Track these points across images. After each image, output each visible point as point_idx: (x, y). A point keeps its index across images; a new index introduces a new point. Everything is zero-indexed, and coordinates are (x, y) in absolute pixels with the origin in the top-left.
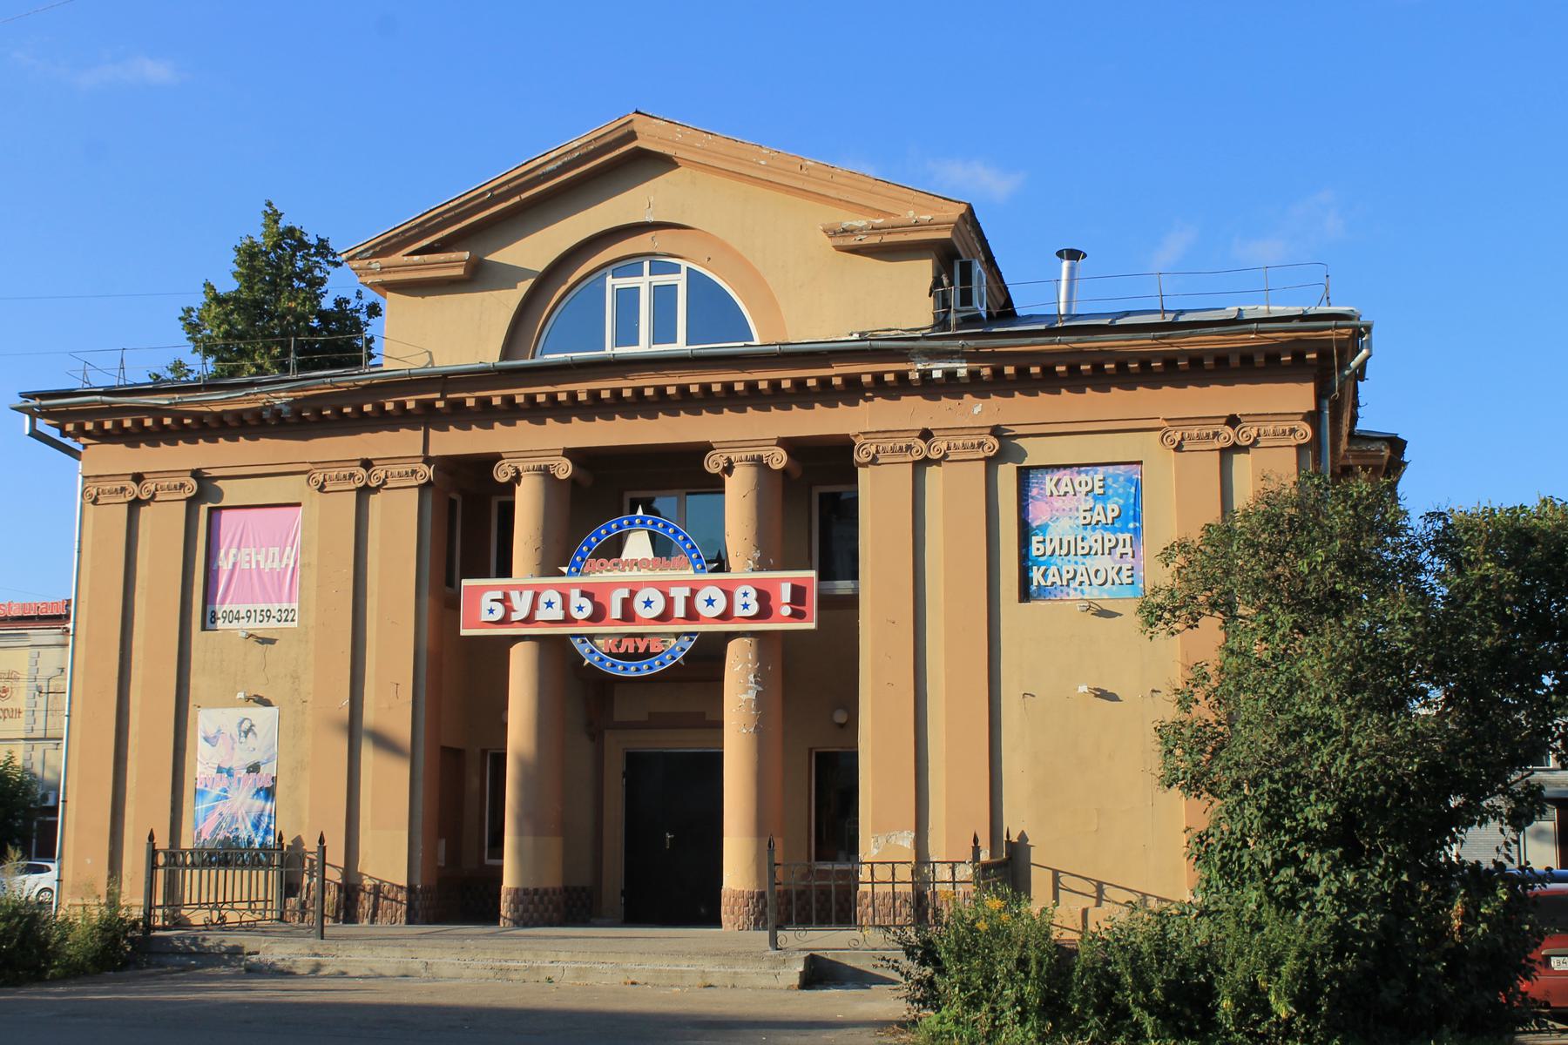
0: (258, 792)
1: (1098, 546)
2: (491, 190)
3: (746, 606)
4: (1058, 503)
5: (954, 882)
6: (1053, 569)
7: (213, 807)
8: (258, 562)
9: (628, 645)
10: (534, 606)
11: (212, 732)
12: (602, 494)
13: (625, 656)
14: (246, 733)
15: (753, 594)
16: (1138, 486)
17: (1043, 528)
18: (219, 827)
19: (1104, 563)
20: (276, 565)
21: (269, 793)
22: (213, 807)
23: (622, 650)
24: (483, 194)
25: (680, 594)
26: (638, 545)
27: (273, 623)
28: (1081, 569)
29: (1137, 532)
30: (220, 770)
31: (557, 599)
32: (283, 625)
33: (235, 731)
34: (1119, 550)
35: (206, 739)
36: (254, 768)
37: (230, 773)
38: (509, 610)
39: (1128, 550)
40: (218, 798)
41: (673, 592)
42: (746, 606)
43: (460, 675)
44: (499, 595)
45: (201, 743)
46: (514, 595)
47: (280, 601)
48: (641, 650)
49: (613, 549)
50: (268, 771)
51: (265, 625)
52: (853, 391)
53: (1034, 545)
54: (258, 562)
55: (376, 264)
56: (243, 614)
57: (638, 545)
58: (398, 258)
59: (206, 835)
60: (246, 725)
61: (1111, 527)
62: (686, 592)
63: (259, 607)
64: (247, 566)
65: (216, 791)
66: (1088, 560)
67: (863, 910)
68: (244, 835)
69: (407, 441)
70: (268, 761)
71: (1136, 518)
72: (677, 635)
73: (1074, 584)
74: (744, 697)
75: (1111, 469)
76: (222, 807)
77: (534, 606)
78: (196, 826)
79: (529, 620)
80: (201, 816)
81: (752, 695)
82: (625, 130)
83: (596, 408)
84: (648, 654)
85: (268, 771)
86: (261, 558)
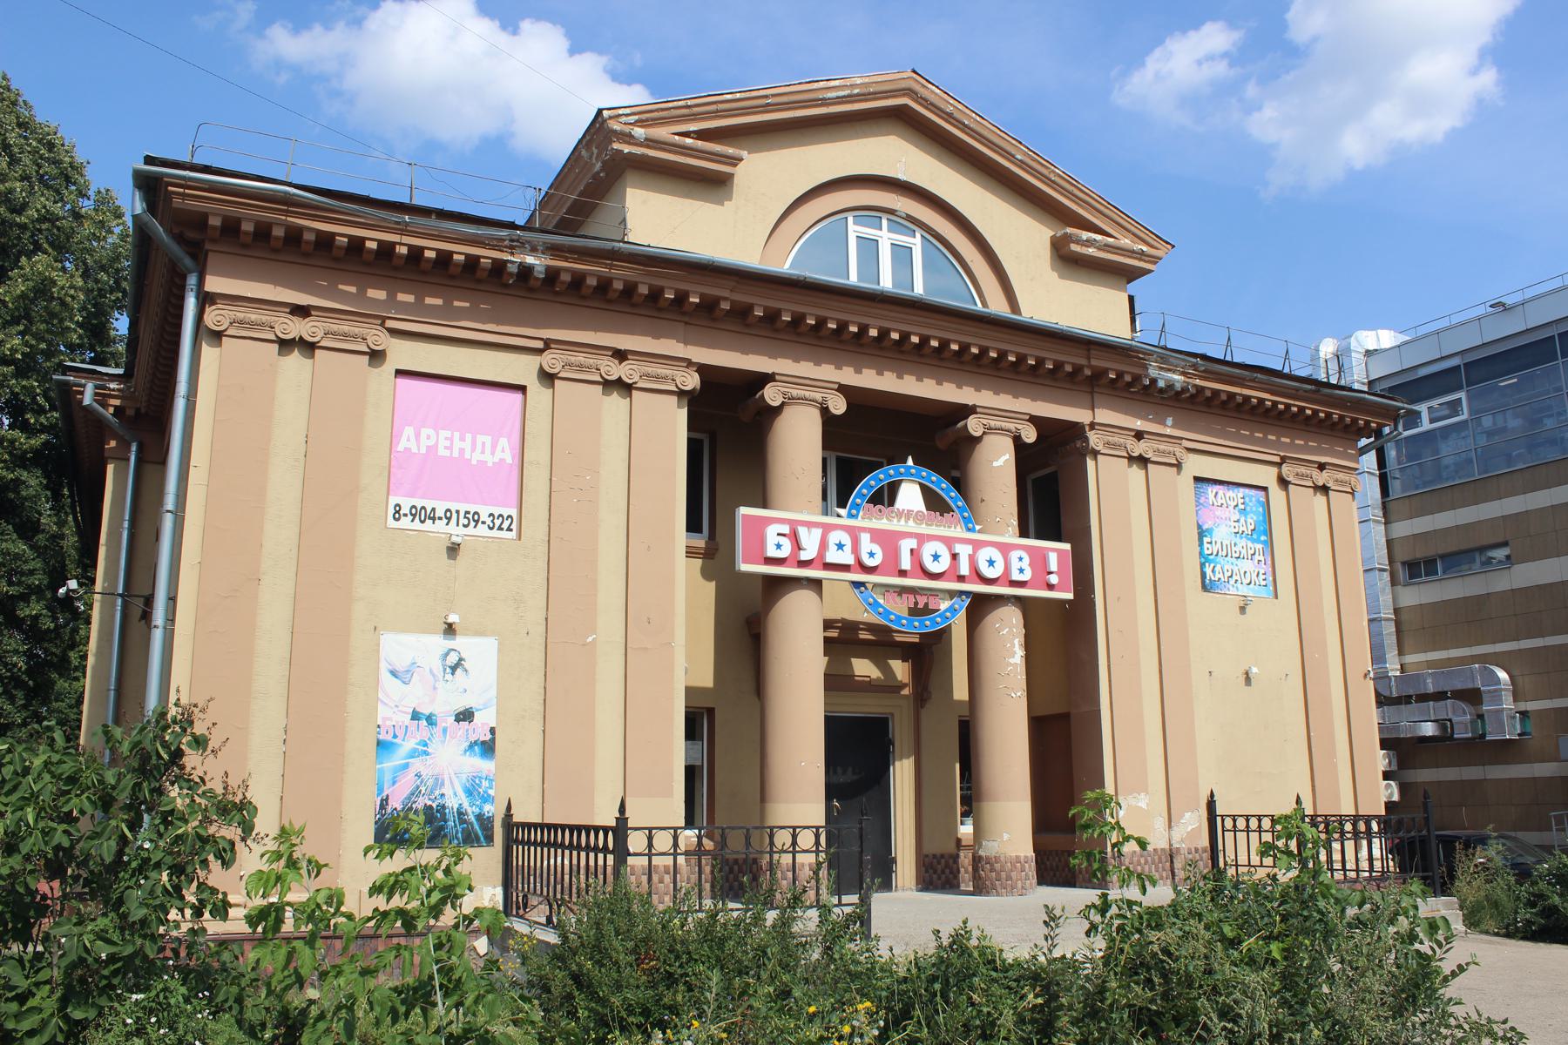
0: (471, 746)
3: (1021, 571)
4: (1219, 512)
5: (650, 855)
6: (1218, 568)
7: (406, 766)
8: (462, 451)
10: (823, 546)
14: (454, 669)
15: (1026, 559)
17: (1210, 531)
18: (416, 792)
19: (1247, 565)
21: (488, 748)
22: (406, 766)
24: (766, 97)
26: (910, 497)
27: (482, 530)
30: (416, 716)
31: (846, 539)
32: (495, 533)
33: (437, 666)
35: (394, 673)
36: (465, 716)
37: (430, 720)
38: (798, 546)
40: (413, 754)
41: (958, 548)
44: (786, 529)
45: (385, 676)
46: (802, 531)
48: (921, 606)
49: (885, 497)
50: (485, 719)
51: (471, 530)
57: (910, 497)
58: (663, 133)
59: (396, 803)
60: (453, 659)
61: (1250, 537)
62: (969, 549)
63: (463, 508)
65: (409, 744)
68: (452, 803)
72: (952, 594)
73: (1232, 581)
75: (1247, 491)
76: (417, 765)
77: (823, 546)
78: (381, 790)
80: (388, 777)
85: (485, 719)
86: (467, 445)
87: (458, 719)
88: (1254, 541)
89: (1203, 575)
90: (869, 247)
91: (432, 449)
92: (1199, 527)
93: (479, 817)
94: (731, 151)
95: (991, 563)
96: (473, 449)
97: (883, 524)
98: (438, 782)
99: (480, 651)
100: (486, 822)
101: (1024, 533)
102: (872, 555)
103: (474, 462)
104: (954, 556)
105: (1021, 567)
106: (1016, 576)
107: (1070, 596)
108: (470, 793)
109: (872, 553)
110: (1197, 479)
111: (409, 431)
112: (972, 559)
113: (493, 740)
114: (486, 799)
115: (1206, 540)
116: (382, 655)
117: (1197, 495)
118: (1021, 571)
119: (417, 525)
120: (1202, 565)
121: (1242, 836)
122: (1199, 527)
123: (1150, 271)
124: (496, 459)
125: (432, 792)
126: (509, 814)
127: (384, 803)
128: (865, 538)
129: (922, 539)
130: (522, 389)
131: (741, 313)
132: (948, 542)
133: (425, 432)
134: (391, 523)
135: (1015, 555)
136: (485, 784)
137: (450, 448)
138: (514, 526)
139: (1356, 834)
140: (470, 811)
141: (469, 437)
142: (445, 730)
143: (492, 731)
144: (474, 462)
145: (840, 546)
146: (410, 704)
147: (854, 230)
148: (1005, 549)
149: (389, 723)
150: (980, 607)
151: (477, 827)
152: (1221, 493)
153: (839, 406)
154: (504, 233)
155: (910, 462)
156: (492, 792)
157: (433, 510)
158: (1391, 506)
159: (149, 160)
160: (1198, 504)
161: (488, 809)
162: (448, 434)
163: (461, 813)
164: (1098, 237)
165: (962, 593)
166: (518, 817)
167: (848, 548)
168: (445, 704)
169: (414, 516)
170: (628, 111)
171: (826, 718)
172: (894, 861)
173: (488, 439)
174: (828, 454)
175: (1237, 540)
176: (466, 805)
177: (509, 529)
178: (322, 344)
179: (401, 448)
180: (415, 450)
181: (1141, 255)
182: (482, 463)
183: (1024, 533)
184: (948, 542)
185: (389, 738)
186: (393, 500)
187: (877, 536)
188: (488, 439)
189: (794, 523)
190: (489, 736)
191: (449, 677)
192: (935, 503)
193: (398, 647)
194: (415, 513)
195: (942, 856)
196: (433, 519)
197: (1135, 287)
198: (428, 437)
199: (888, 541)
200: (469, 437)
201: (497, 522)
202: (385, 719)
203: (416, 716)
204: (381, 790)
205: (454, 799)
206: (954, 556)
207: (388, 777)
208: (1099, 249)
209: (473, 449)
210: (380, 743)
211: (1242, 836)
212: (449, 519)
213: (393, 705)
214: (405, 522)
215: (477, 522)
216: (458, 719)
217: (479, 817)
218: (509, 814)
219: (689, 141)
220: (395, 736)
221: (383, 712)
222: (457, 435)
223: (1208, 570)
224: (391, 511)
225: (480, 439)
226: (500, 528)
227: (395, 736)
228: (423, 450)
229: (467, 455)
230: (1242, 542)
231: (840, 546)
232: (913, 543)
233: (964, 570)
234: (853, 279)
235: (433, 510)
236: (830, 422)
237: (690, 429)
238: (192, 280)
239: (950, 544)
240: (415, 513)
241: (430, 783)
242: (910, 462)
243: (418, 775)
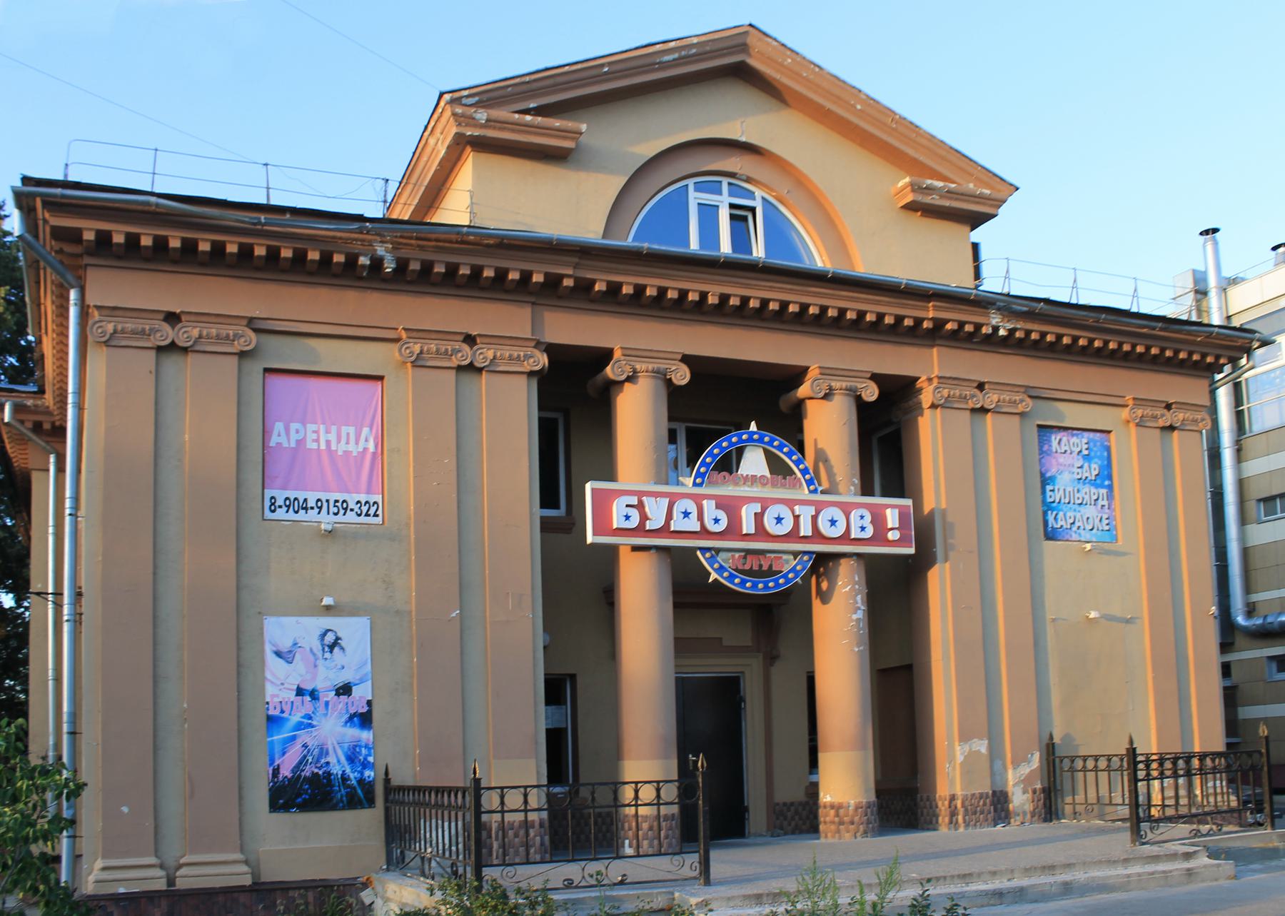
0: (351, 718)
1: (1087, 497)
2: (610, 64)
4: (1062, 459)
6: (1061, 515)
7: (294, 738)
8: (328, 442)
9: (752, 563)
10: (669, 516)
11: (285, 645)
12: (724, 409)
13: (750, 573)
14: (332, 647)
15: (868, 517)
16: (1108, 449)
17: (1052, 479)
18: (303, 761)
19: (1090, 511)
20: (351, 447)
21: (365, 720)
22: (294, 738)
23: (747, 567)
24: (602, 65)
25: (806, 513)
26: (754, 462)
28: (1078, 516)
29: (1110, 488)
30: (300, 692)
31: (692, 508)
32: (363, 519)
33: (317, 645)
34: (1100, 503)
35: (278, 654)
36: (345, 690)
37: (314, 695)
38: (644, 518)
39: (1105, 502)
40: (300, 726)
42: (863, 529)
43: (578, 587)
44: (634, 500)
45: (271, 659)
47: (369, 492)
48: (765, 568)
49: (728, 464)
50: (362, 692)
51: (340, 518)
52: (936, 335)
53: (1049, 493)
54: (328, 442)
55: (482, 116)
56: (311, 503)
58: (501, 113)
59: (286, 772)
60: (330, 638)
61: (1094, 483)
62: (811, 510)
63: (333, 496)
64: (314, 446)
65: (296, 718)
66: (1082, 509)
67: (826, 816)
68: (336, 770)
69: (511, 319)
70: (362, 681)
71: (1110, 477)
72: (795, 554)
73: (1074, 528)
74: (855, 617)
75: (1091, 435)
76: (304, 737)
77: (669, 516)
78: (272, 761)
79: (664, 531)
80: (278, 749)
81: (860, 615)
82: (740, 41)
83: (724, 313)
84: (770, 573)
85: (362, 692)
87: (338, 693)
88: (1097, 486)
89: (1046, 523)
90: (708, 213)
91: (301, 442)
92: (1042, 475)
93: (361, 781)
94: (569, 124)
95: (832, 523)
96: (339, 441)
97: (728, 490)
98: (323, 752)
99: (354, 631)
100: (368, 787)
101: (866, 490)
102: (717, 521)
103: (340, 453)
104: (797, 518)
105: (860, 524)
106: (854, 534)
107: (912, 551)
108: (351, 759)
109: (715, 519)
110: (1039, 426)
111: (279, 426)
112: (815, 519)
113: (370, 712)
114: (365, 765)
115: (1049, 488)
116: (267, 637)
117: (1041, 443)
118: (863, 529)
119: (291, 515)
120: (1045, 514)
121: (1103, 776)
122: (1042, 475)
123: (994, 216)
124: (361, 449)
125: (318, 761)
126: (387, 780)
127: (276, 772)
128: (709, 506)
129: (766, 503)
130: (381, 378)
131: (584, 288)
132: (790, 503)
133: (294, 426)
134: (268, 515)
135: (854, 515)
136: (364, 751)
137: (317, 441)
138: (380, 512)
139: (1189, 774)
140: (352, 776)
141: (334, 429)
142: (327, 704)
143: (369, 703)
144: (340, 453)
145: (686, 514)
146: (294, 682)
147: (695, 198)
148: (846, 509)
149: (277, 700)
150: (823, 563)
151: (359, 791)
152: (1064, 439)
153: (682, 376)
154: (355, 226)
155: (753, 427)
156: (371, 759)
157: (305, 500)
158: (1247, 443)
159: (26, 180)
160: (1041, 452)
161: (369, 774)
162: (314, 427)
163: (345, 778)
164: (940, 184)
165: (805, 553)
166: (396, 781)
167: (694, 515)
168: (325, 679)
169: (288, 507)
170: (466, 93)
171: (677, 679)
172: (746, 809)
173: (352, 430)
174: (675, 425)
175: (1080, 486)
176: (348, 771)
177: (376, 515)
178: (197, 348)
179: (272, 444)
180: (285, 445)
181: (981, 198)
182: (347, 453)
183: (866, 490)
184: (790, 503)
185: (277, 713)
186: (269, 493)
187: (722, 504)
188: (352, 430)
189: (642, 493)
190: (365, 709)
191: (327, 655)
192: (776, 466)
193: (281, 630)
194: (289, 504)
195: (792, 804)
196: (306, 509)
197: (977, 235)
198: (297, 432)
199: (730, 506)
200: (334, 429)
201: (365, 509)
202: (273, 696)
203: (300, 692)
204: (272, 761)
205: (338, 765)
206: (797, 518)
207: (278, 749)
208: (942, 197)
209: (339, 441)
210: (271, 719)
211: (1091, 776)
212: (320, 508)
213: (278, 683)
214: (280, 514)
215: (346, 509)
216: (338, 693)
217: (361, 781)
218: (387, 780)
219: (528, 118)
220: (282, 712)
221: (270, 690)
222: (322, 428)
223: (1051, 518)
224: (267, 504)
225: (344, 430)
226: (367, 515)
227: (282, 712)
228: (293, 444)
229: (333, 448)
230: (1086, 489)
231: (686, 514)
232: (757, 508)
233: (806, 530)
234: (694, 245)
235: (305, 500)
236: (675, 396)
237: (541, 408)
238: (73, 295)
239: (791, 503)
240: (289, 504)
241: (316, 752)
242: (753, 427)
243: (305, 746)
